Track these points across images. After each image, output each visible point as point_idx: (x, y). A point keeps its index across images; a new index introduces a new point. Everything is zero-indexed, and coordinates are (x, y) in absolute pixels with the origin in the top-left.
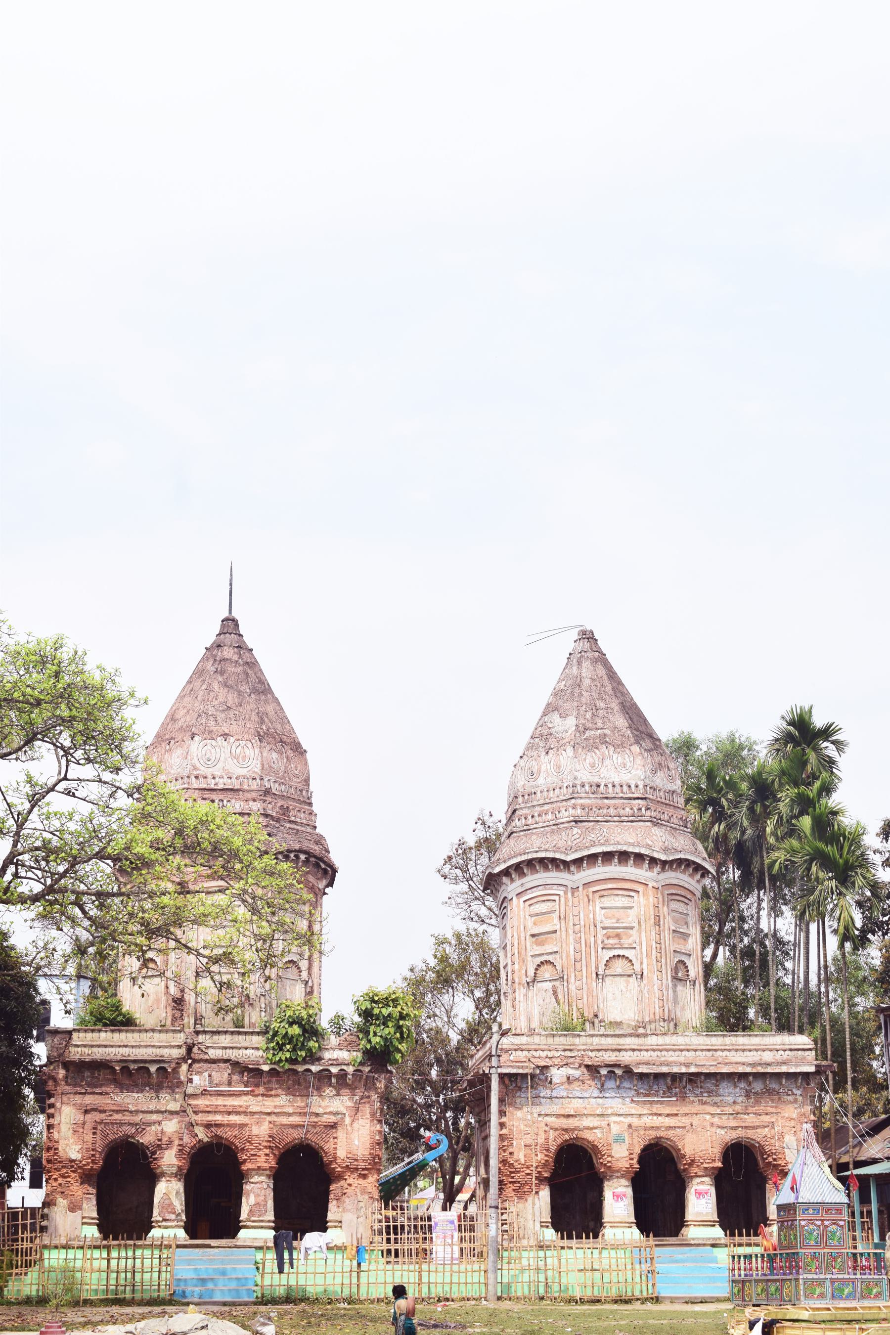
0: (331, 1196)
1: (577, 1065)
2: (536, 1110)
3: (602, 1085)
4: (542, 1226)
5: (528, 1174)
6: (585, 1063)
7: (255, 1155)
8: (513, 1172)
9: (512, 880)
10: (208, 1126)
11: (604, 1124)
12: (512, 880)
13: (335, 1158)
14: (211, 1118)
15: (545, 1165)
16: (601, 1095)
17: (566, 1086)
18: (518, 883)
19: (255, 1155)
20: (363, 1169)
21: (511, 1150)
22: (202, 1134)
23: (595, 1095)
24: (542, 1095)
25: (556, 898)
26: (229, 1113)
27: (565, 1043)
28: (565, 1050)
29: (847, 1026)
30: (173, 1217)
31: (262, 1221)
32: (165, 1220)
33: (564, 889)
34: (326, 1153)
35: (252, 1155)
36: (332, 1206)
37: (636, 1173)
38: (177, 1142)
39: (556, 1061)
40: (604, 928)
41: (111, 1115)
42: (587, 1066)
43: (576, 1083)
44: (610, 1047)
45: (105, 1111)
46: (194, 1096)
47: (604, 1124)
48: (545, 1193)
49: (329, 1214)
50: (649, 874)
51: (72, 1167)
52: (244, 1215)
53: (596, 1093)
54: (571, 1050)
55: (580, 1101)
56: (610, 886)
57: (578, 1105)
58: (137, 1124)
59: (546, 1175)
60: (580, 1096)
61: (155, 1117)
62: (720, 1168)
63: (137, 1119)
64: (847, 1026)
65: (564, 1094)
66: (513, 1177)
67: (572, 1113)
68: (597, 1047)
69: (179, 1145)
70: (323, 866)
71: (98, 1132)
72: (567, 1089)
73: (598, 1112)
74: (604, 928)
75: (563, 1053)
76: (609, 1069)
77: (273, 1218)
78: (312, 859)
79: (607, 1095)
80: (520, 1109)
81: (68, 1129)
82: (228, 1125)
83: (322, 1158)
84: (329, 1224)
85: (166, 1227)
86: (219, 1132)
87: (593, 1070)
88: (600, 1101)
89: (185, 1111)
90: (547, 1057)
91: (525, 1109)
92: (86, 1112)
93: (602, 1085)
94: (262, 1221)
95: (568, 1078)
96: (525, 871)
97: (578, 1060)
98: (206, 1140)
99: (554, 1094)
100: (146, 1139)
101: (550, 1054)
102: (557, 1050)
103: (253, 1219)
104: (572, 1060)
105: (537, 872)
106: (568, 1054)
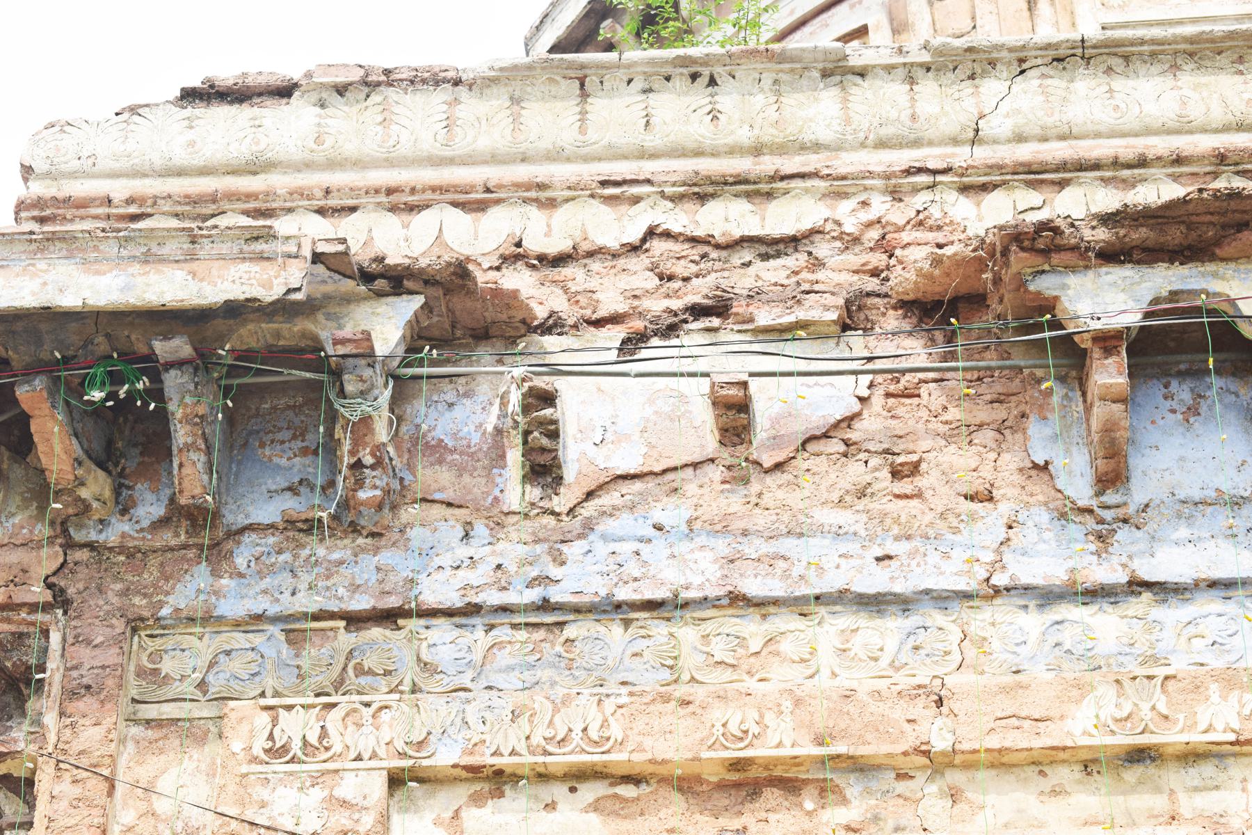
1: (823, 310)
2: (379, 732)
3: (1112, 477)
6: (903, 279)
16: (1109, 573)
17: (708, 494)
23: (1048, 556)
24: (439, 590)
27: (699, 130)
28: (701, 191)
39: (610, 290)
42: (934, 311)
43: (828, 474)
44: (1160, 145)
53: (1048, 556)
54: (757, 190)
55: (888, 631)
57: (861, 679)
60: (874, 581)
65: (699, 571)
67: (782, 740)
68: (1026, 152)
72: (721, 527)
73: (1087, 723)
75: (677, 219)
76: (1163, 279)
79: (1168, 563)
80: (192, 733)
87: (984, 315)
88: (1105, 626)
90: (515, 256)
91: (248, 726)
93: (1112, 477)
95: (734, 414)
97: (840, 273)
99: (580, 577)
101: (545, 232)
102: (614, 192)
104: (774, 272)
106: (728, 217)
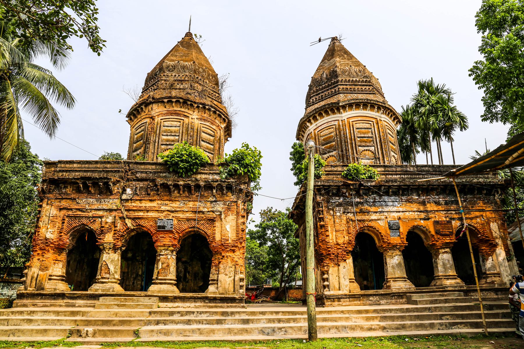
0: (213, 264)
4: (350, 282)
5: (339, 249)
7: (163, 237)
8: (330, 248)
9: (311, 124)
10: (134, 219)
11: (383, 217)
12: (311, 124)
13: (214, 238)
14: (137, 214)
15: (349, 243)
18: (314, 124)
19: (163, 237)
20: (233, 246)
21: (327, 234)
22: (129, 223)
25: (334, 126)
26: (148, 211)
29: (458, 195)
30: (108, 276)
31: (165, 280)
32: (103, 278)
33: (337, 122)
34: (209, 236)
35: (161, 237)
36: (213, 270)
37: (406, 247)
38: (113, 229)
40: (359, 137)
41: (75, 212)
45: (71, 209)
46: (127, 200)
47: (383, 217)
48: (350, 261)
49: (211, 275)
50: (377, 114)
51: (47, 243)
52: (154, 277)
56: (360, 119)
58: (90, 217)
59: (350, 249)
61: (100, 213)
62: (454, 243)
63: (90, 214)
64: (458, 195)
66: (329, 251)
69: (115, 230)
70: (223, 117)
71: (66, 222)
74: (359, 137)
77: (174, 278)
78: (218, 112)
81: (51, 223)
82: (147, 218)
83: (207, 240)
84: (210, 282)
85: (103, 283)
86: (142, 222)
89: (120, 210)
92: (61, 209)
94: (165, 280)
96: (318, 118)
98: (132, 228)
100: (95, 227)
103: (159, 278)
105: (323, 117)
